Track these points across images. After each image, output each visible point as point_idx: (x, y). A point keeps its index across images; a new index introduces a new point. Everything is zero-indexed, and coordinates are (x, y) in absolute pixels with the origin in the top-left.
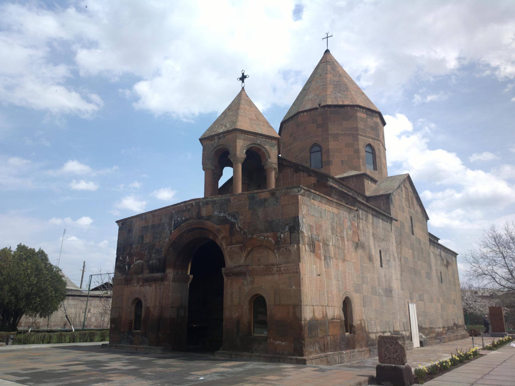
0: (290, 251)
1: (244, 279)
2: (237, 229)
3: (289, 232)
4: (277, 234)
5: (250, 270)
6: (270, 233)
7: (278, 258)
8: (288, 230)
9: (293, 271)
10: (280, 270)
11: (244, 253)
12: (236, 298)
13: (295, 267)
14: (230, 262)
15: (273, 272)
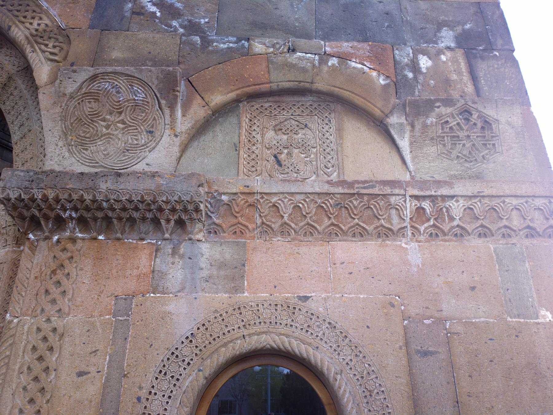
0: (487, 124)
1: (169, 249)
2: (143, 7)
3: (460, 53)
4: (397, 52)
5: (224, 198)
6: (356, 44)
7: (408, 158)
8: (453, 45)
9: (531, 225)
10: (439, 214)
11: (179, 113)
12: (80, 374)
13: (539, 202)
14: (67, 154)
15: (389, 220)
